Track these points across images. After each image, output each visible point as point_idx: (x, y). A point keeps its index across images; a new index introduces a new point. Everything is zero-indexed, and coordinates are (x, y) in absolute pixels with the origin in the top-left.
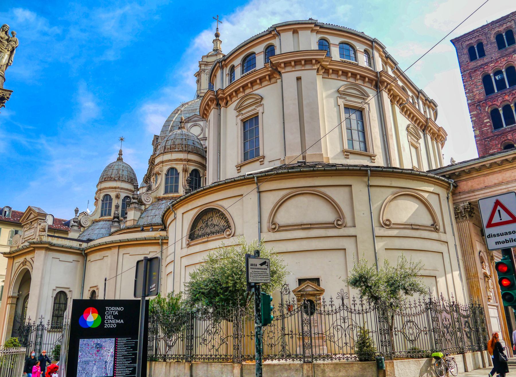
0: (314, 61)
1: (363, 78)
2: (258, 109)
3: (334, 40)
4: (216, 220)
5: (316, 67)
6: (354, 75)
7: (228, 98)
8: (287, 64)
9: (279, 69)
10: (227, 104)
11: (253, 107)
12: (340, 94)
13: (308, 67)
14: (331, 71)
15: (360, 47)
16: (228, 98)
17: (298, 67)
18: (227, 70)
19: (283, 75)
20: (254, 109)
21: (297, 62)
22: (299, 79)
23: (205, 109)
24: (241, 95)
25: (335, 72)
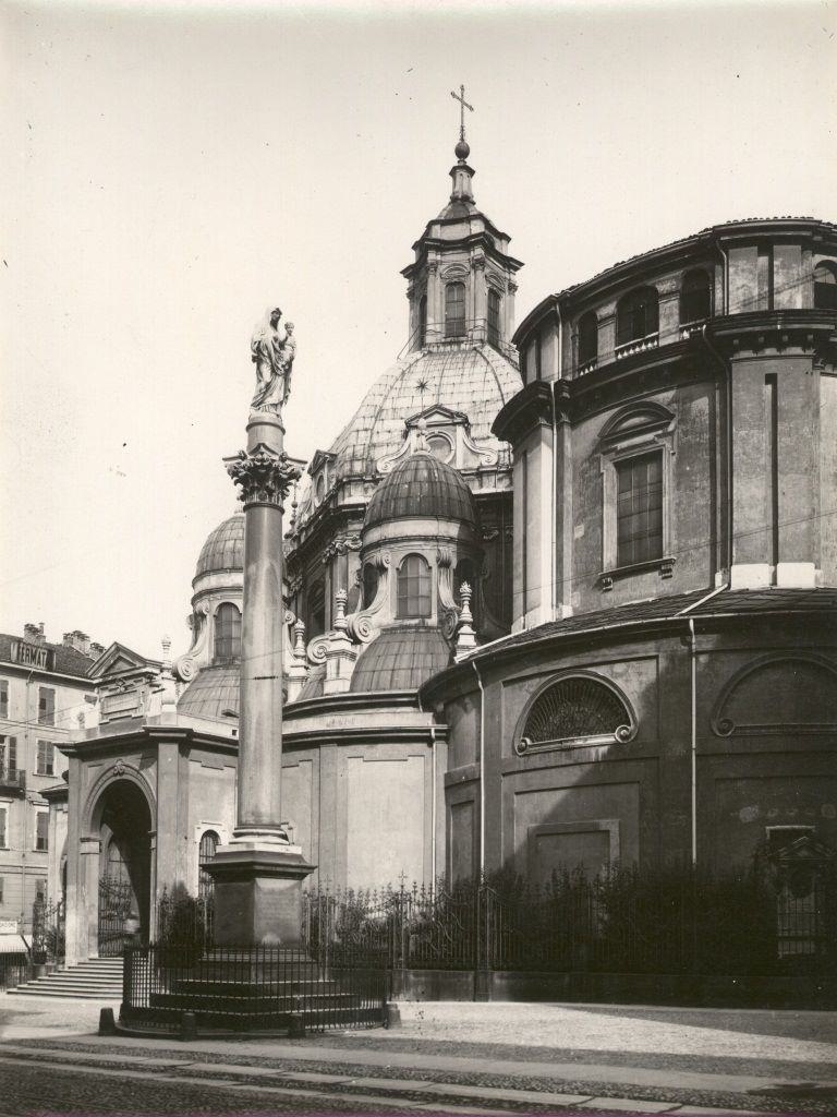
11: (649, 437)
20: (652, 442)
21: (777, 340)
22: (771, 379)
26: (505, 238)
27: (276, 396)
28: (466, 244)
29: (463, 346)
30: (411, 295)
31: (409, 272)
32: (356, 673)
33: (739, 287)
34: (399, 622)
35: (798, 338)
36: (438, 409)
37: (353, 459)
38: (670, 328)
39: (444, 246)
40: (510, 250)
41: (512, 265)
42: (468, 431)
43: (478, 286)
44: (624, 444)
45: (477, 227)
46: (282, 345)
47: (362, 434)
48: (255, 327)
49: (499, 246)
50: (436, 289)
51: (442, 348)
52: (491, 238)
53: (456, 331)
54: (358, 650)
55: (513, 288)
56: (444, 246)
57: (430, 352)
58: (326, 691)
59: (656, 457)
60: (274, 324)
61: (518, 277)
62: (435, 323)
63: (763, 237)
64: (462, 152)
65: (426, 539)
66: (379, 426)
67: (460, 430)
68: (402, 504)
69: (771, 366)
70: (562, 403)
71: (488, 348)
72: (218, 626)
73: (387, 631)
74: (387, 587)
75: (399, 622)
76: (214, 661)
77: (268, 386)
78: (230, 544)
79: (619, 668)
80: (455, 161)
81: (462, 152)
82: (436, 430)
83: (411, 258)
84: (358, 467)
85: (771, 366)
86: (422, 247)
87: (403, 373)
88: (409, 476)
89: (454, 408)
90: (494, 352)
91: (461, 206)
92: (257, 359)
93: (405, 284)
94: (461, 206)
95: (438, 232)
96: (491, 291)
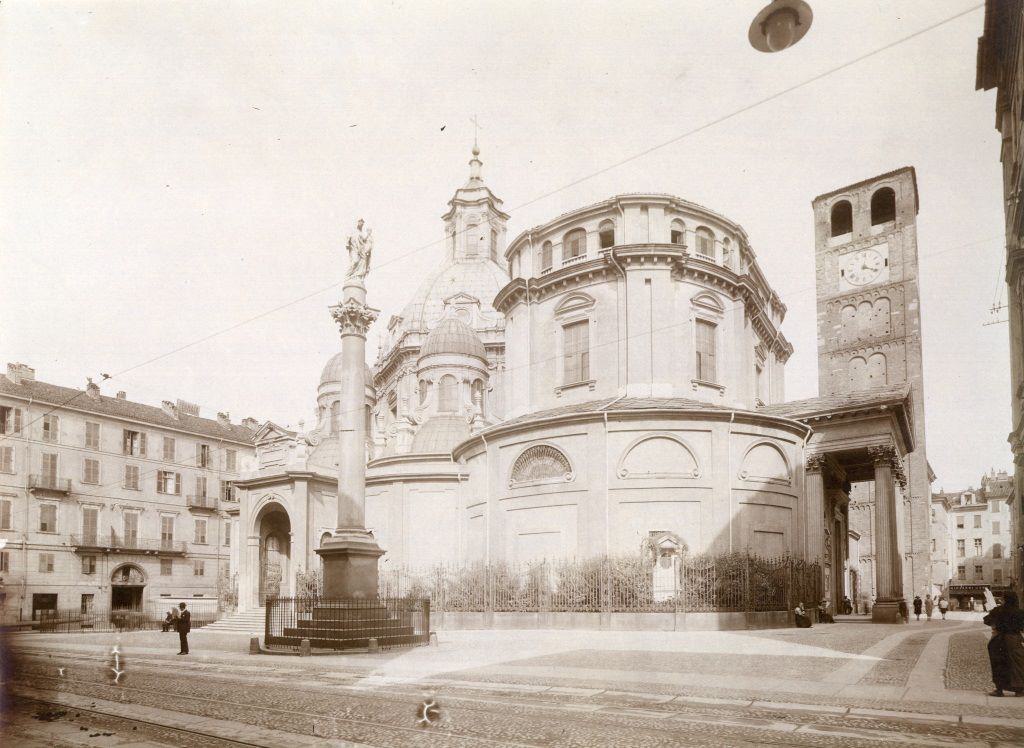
0: (669, 260)
1: (721, 281)
2: (588, 314)
3: (692, 224)
4: (548, 461)
5: (669, 267)
6: (711, 278)
7: (544, 292)
8: (636, 259)
9: (624, 265)
10: (539, 299)
12: (693, 304)
13: (662, 266)
14: (685, 271)
15: (720, 235)
16: (544, 292)
17: (648, 266)
18: (539, 247)
19: (628, 273)
21: (649, 258)
23: (506, 301)
24: (561, 291)
25: (691, 272)
26: (499, 201)
27: (361, 270)
28: (478, 203)
29: (476, 261)
31: (448, 217)
32: (414, 442)
33: (630, 230)
34: (440, 414)
35: (662, 258)
36: (462, 295)
38: (592, 250)
39: (465, 204)
41: (502, 216)
43: (484, 229)
44: (566, 315)
45: (484, 194)
46: (365, 241)
48: (349, 230)
49: (498, 206)
50: (461, 225)
51: (465, 261)
52: (492, 201)
54: (415, 428)
55: (505, 229)
56: (465, 204)
59: (587, 321)
60: (360, 228)
61: (508, 224)
63: (644, 205)
64: (476, 153)
65: (455, 366)
66: (429, 303)
67: (475, 306)
69: (647, 274)
70: (534, 291)
71: (491, 261)
74: (432, 393)
77: (356, 265)
80: (472, 157)
81: (476, 153)
82: (462, 306)
83: (448, 209)
84: (416, 326)
85: (647, 274)
86: (454, 203)
88: (445, 331)
89: (472, 294)
90: (493, 264)
92: (349, 248)
93: (445, 224)
95: (462, 196)
96: (493, 231)
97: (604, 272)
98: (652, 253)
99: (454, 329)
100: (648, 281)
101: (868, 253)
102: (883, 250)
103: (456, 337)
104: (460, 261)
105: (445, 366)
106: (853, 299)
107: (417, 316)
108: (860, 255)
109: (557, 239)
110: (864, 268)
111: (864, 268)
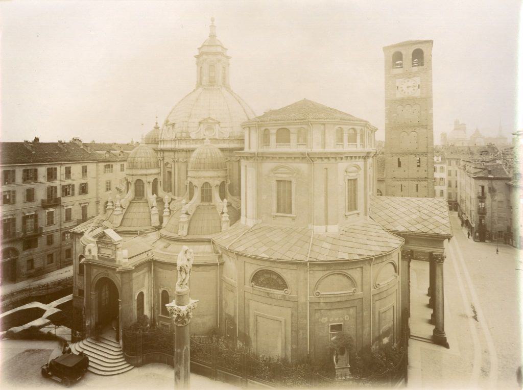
7: (265, 158)
10: (262, 160)
26: (227, 49)
30: (197, 64)
31: (197, 57)
34: (202, 204)
37: (182, 132)
39: (207, 54)
40: (228, 53)
41: (228, 58)
42: (220, 125)
47: (185, 123)
53: (212, 82)
57: (205, 88)
58: (179, 234)
62: (205, 79)
65: (211, 178)
67: (217, 125)
68: (202, 166)
72: (136, 187)
73: (198, 208)
75: (202, 204)
76: (135, 198)
78: (140, 159)
79: (284, 270)
83: (197, 54)
87: (197, 99)
91: (212, 36)
94: (212, 36)
95: (205, 50)
97: (301, 158)
98: (329, 156)
99: (209, 155)
100: (327, 169)
101: (410, 80)
102: (418, 80)
103: (210, 159)
104: (206, 88)
105: (204, 177)
106: (403, 102)
107: (184, 129)
108: (406, 81)
109: (273, 131)
110: (408, 87)
111: (408, 87)
